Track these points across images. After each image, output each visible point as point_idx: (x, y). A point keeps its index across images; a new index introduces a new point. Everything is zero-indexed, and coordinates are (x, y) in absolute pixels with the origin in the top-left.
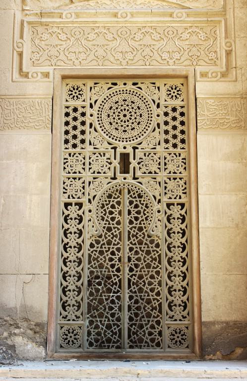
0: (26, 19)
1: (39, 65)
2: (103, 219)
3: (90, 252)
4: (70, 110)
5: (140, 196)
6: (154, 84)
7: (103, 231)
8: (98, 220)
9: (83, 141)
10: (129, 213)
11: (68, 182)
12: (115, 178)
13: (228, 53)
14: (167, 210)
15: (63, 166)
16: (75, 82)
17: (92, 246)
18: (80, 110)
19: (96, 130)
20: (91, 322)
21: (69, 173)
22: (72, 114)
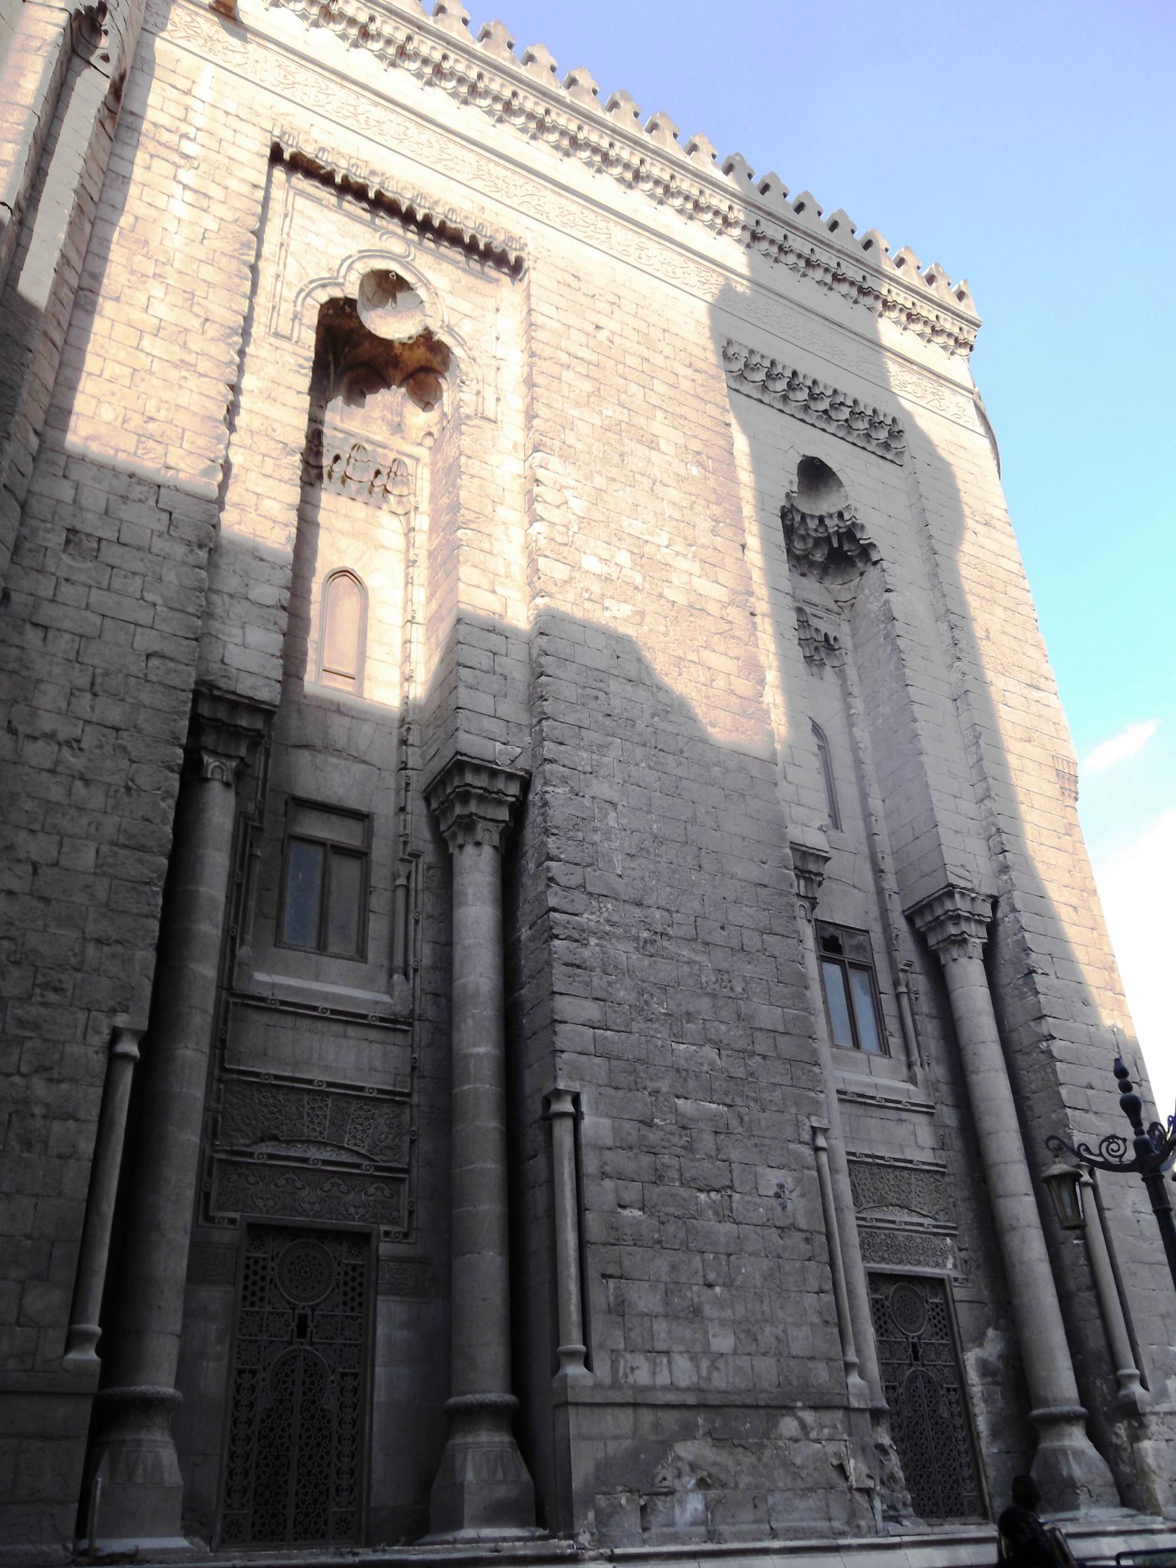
0: (217, 1156)
1: (225, 1210)
2: (276, 1389)
4: (251, 1262)
5: (315, 1365)
9: (262, 1299)
10: (304, 1383)
12: (290, 1343)
13: (411, 1213)
16: (258, 1232)
17: (263, 1421)
18: (261, 1263)
19: (276, 1286)
20: (256, 1512)
22: (253, 1268)
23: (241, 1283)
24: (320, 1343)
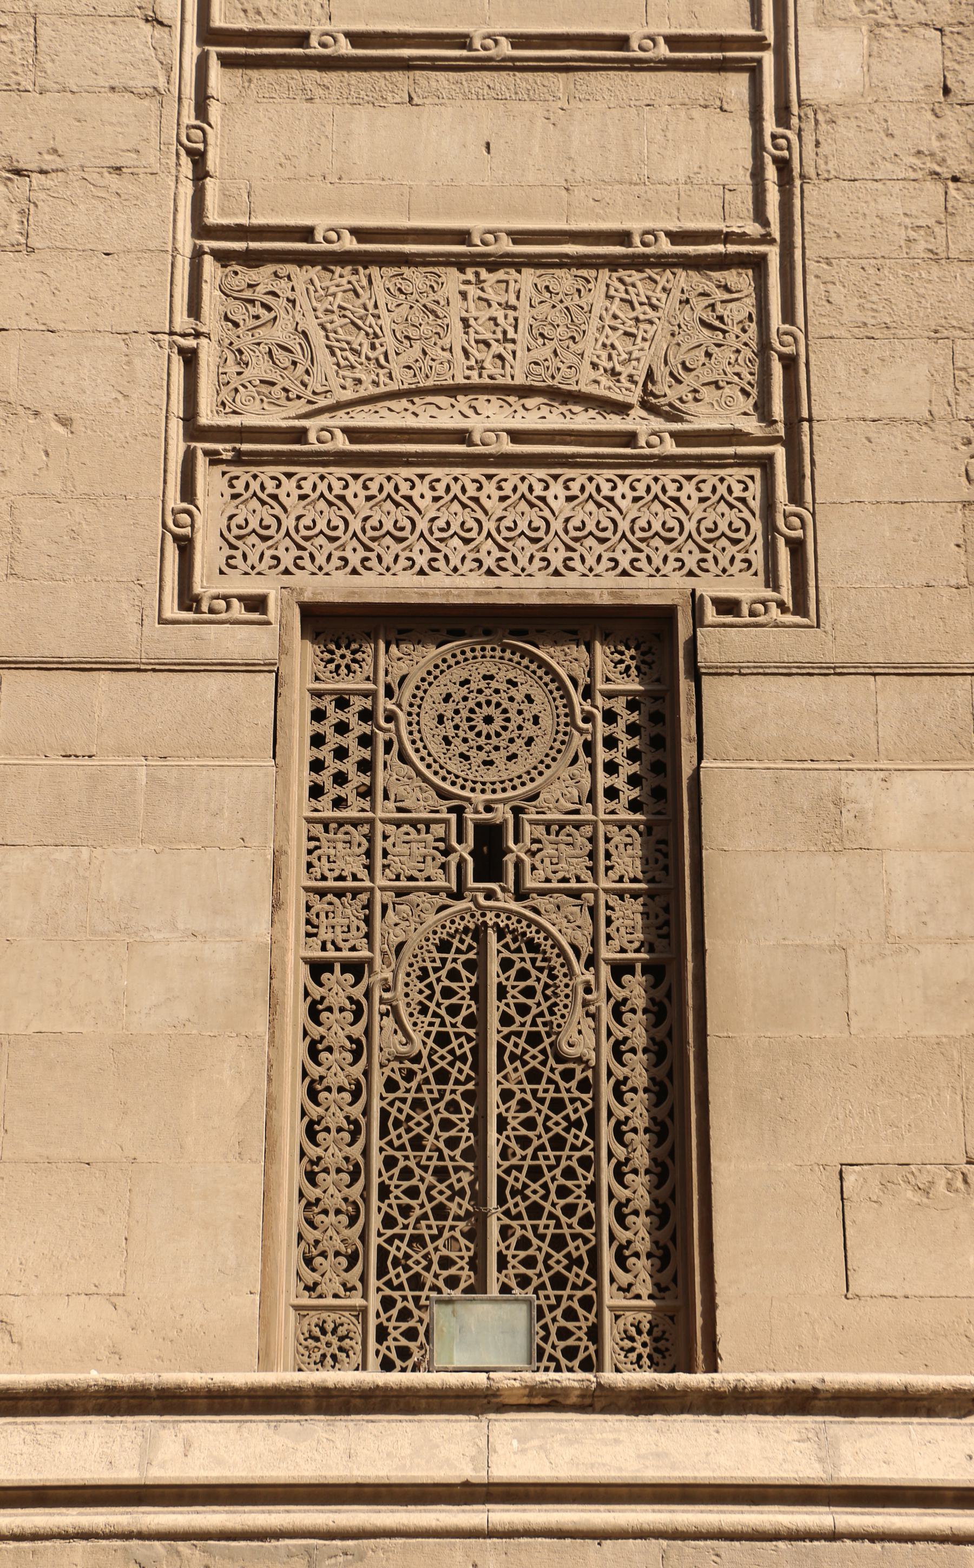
2: (424, 1010)
3: (384, 1104)
6: (575, 632)
7: (424, 1043)
8: (411, 1015)
11: (319, 905)
12: (458, 895)
14: (614, 987)
15: (305, 858)
17: (391, 1085)
21: (324, 878)
23: (299, 753)
24: (542, 893)
